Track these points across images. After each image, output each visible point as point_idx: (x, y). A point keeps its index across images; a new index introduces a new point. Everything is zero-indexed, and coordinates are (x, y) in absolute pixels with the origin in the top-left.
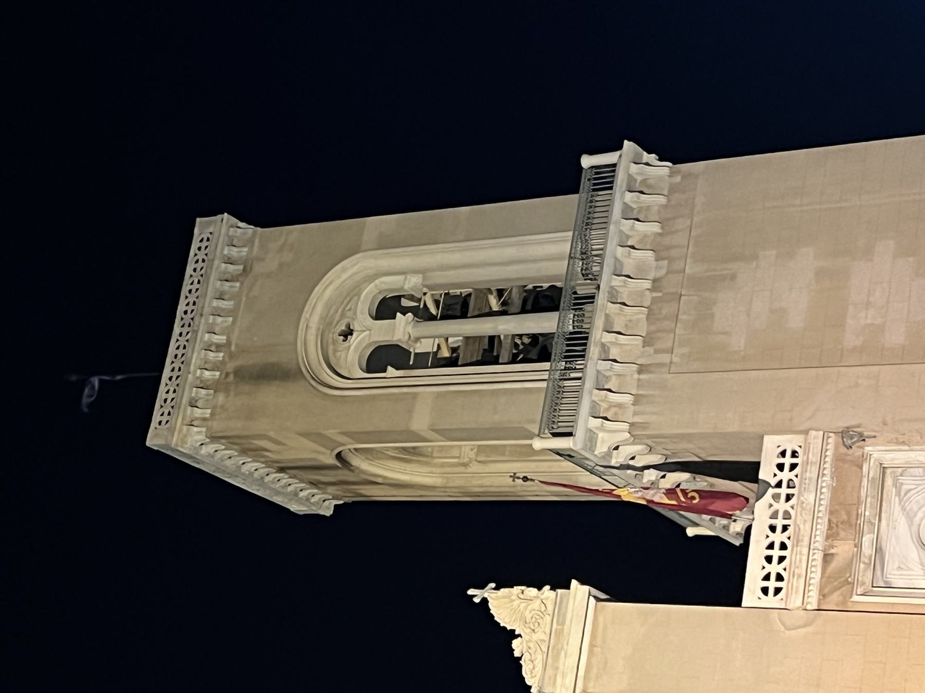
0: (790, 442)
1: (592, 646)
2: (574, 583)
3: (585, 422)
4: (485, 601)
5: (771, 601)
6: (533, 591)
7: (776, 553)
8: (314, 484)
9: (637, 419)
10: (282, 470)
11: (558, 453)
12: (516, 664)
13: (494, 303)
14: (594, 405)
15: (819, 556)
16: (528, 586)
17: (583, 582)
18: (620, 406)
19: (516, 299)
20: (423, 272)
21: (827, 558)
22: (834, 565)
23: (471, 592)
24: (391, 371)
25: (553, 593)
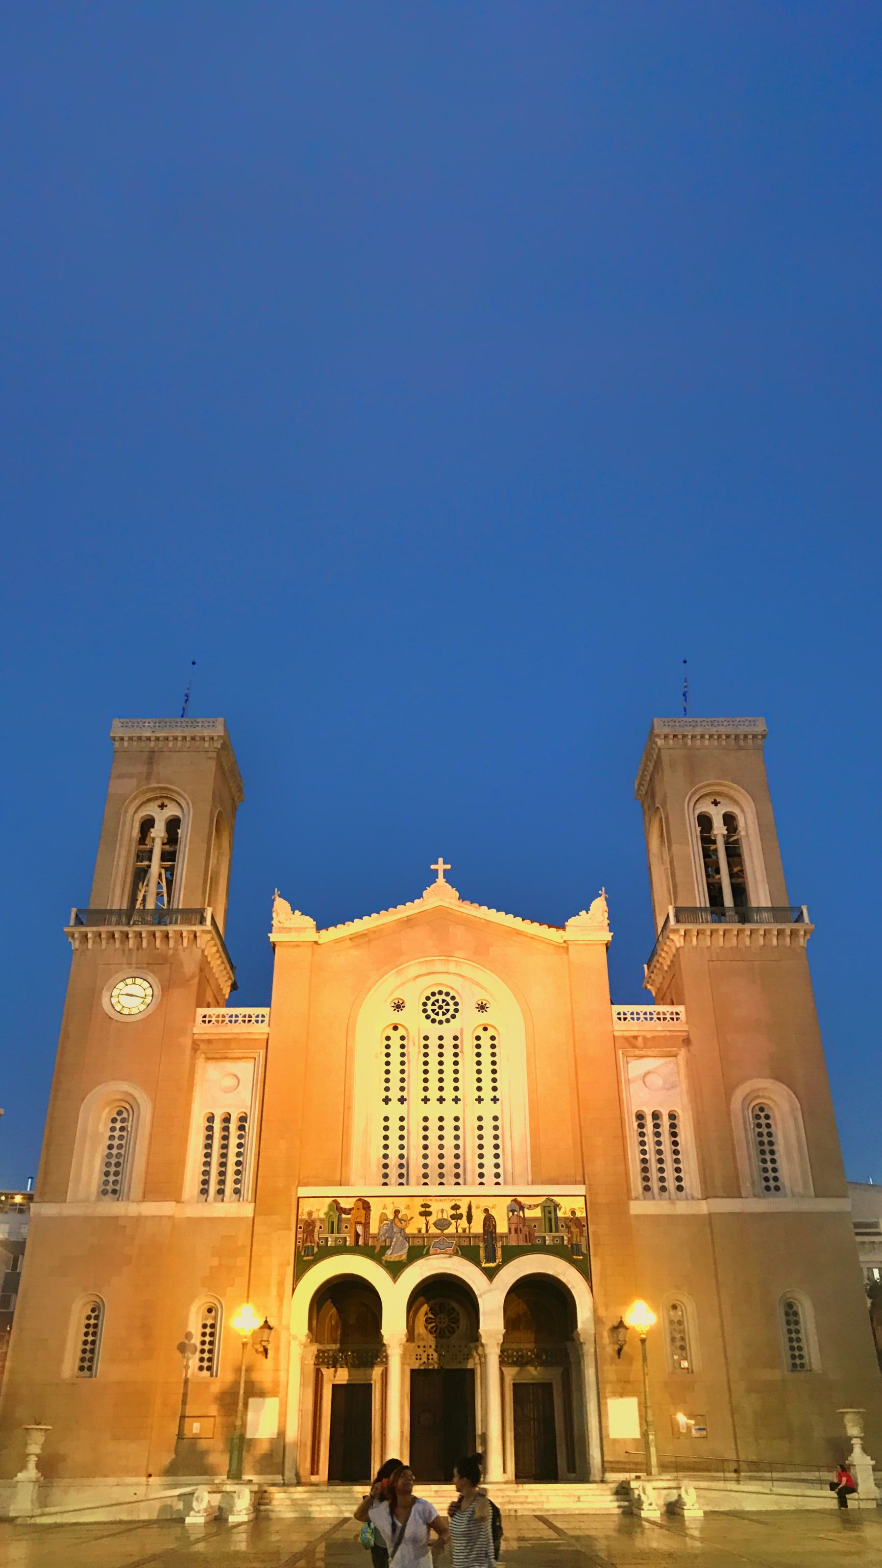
0: (682, 1016)
1: (588, 945)
2: (612, 934)
3: (682, 928)
4: (600, 895)
5: (615, 1016)
6: (606, 915)
7: (635, 1016)
8: (647, 793)
9: (686, 950)
10: (651, 779)
11: (668, 917)
12: (576, 914)
13: (736, 870)
14: (690, 930)
15: (636, 1034)
16: (609, 913)
17: (612, 937)
18: (691, 941)
19: (740, 880)
20: (747, 835)
21: (636, 1037)
22: (633, 1040)
23: (603, 889)
24: (699, 829)
25: (606, 924)
